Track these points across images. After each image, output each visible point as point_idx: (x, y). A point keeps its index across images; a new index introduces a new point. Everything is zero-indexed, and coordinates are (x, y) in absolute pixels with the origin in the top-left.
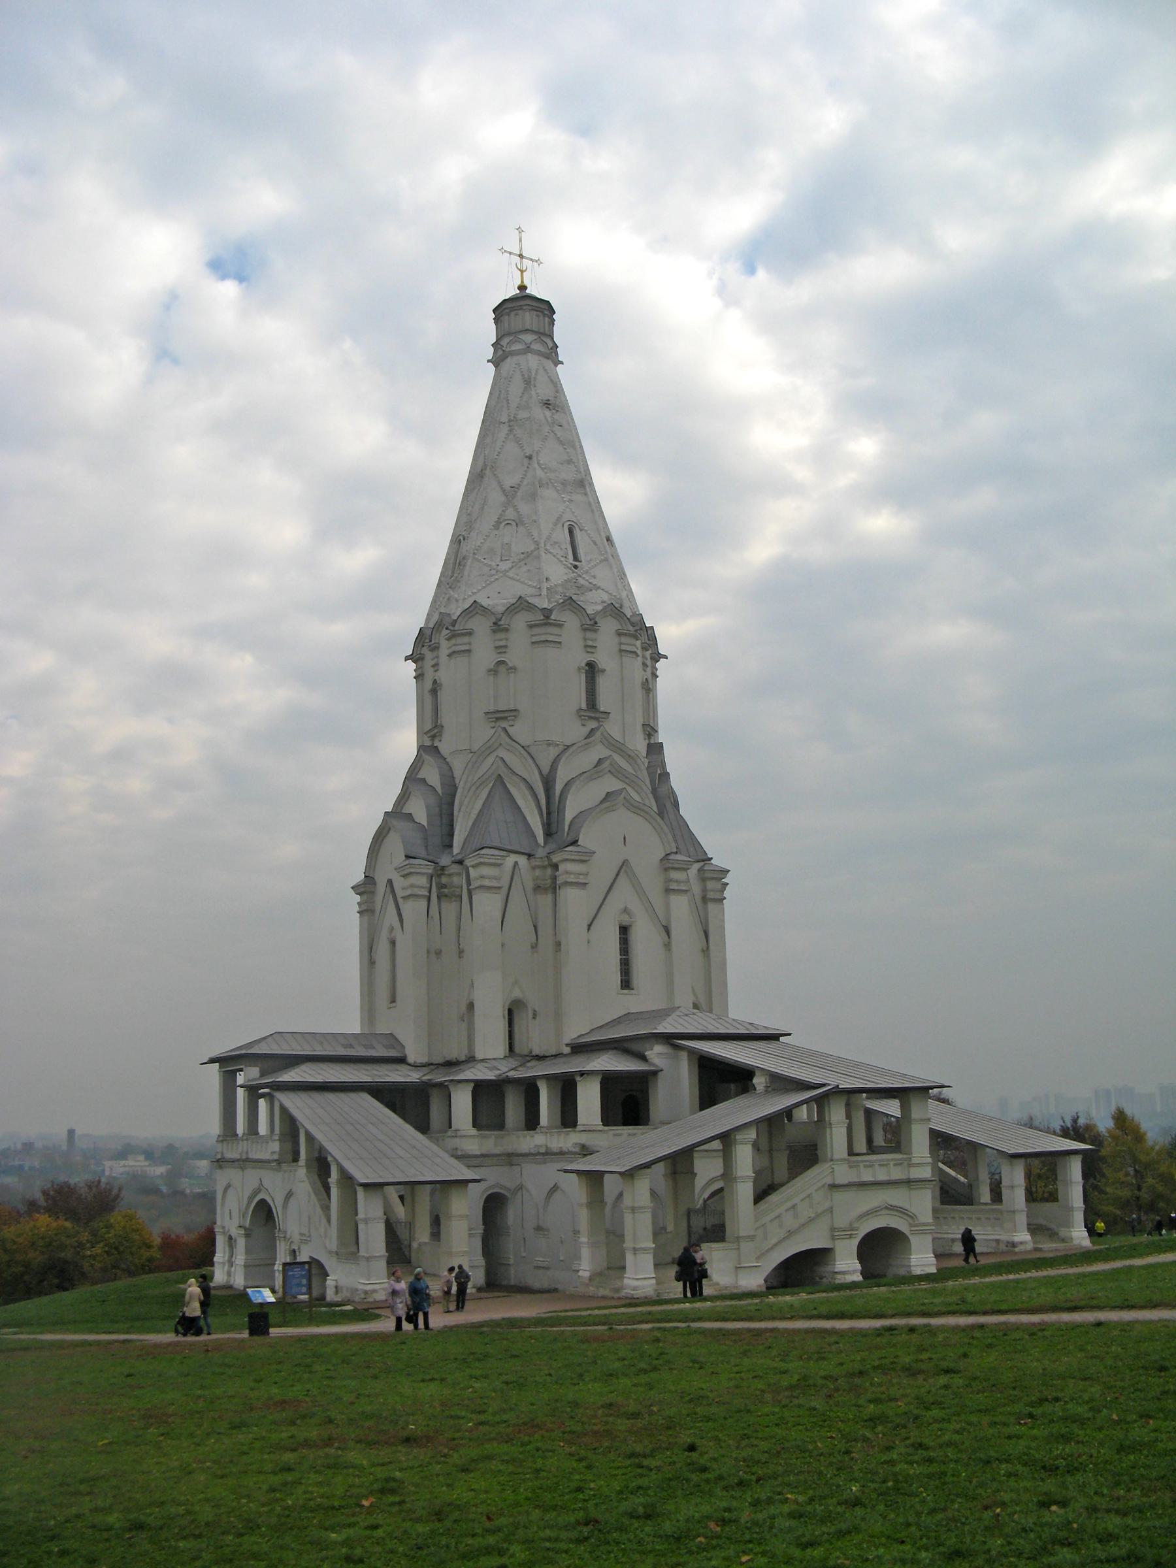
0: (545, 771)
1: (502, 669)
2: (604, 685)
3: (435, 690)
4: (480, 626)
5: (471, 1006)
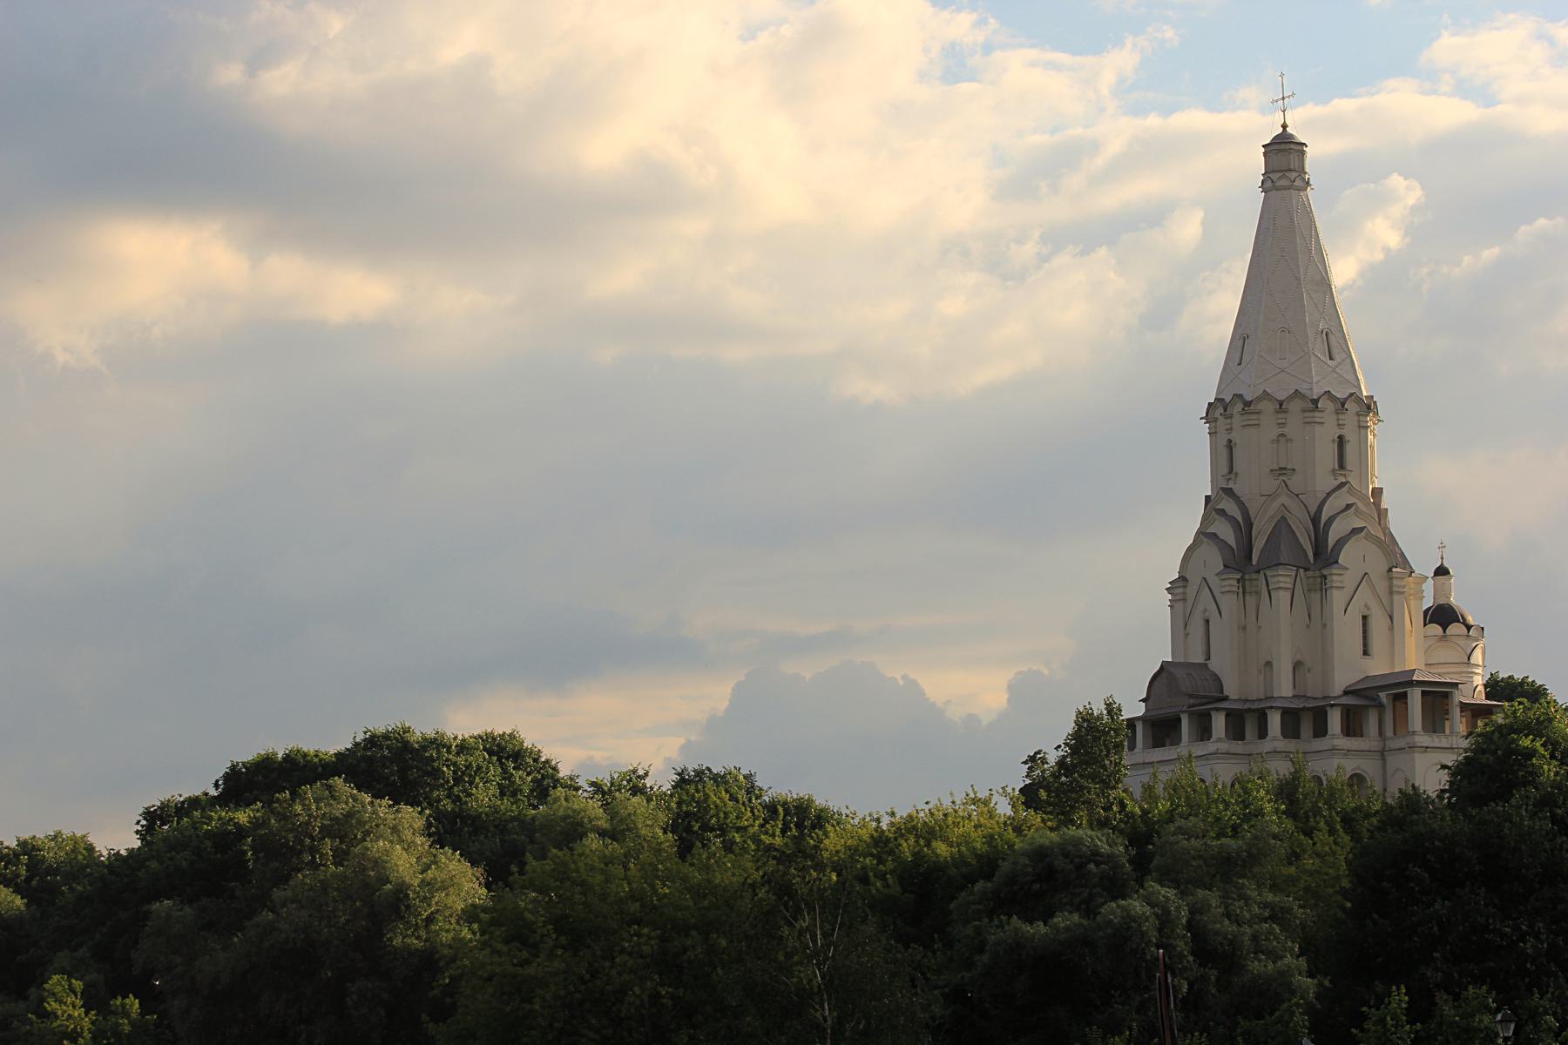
0: (1313, 510)
1: (1282, 440)
2: (1350, 450)
3: (1230, 445)
4: (1267, 407)
5: (1269, 664)
